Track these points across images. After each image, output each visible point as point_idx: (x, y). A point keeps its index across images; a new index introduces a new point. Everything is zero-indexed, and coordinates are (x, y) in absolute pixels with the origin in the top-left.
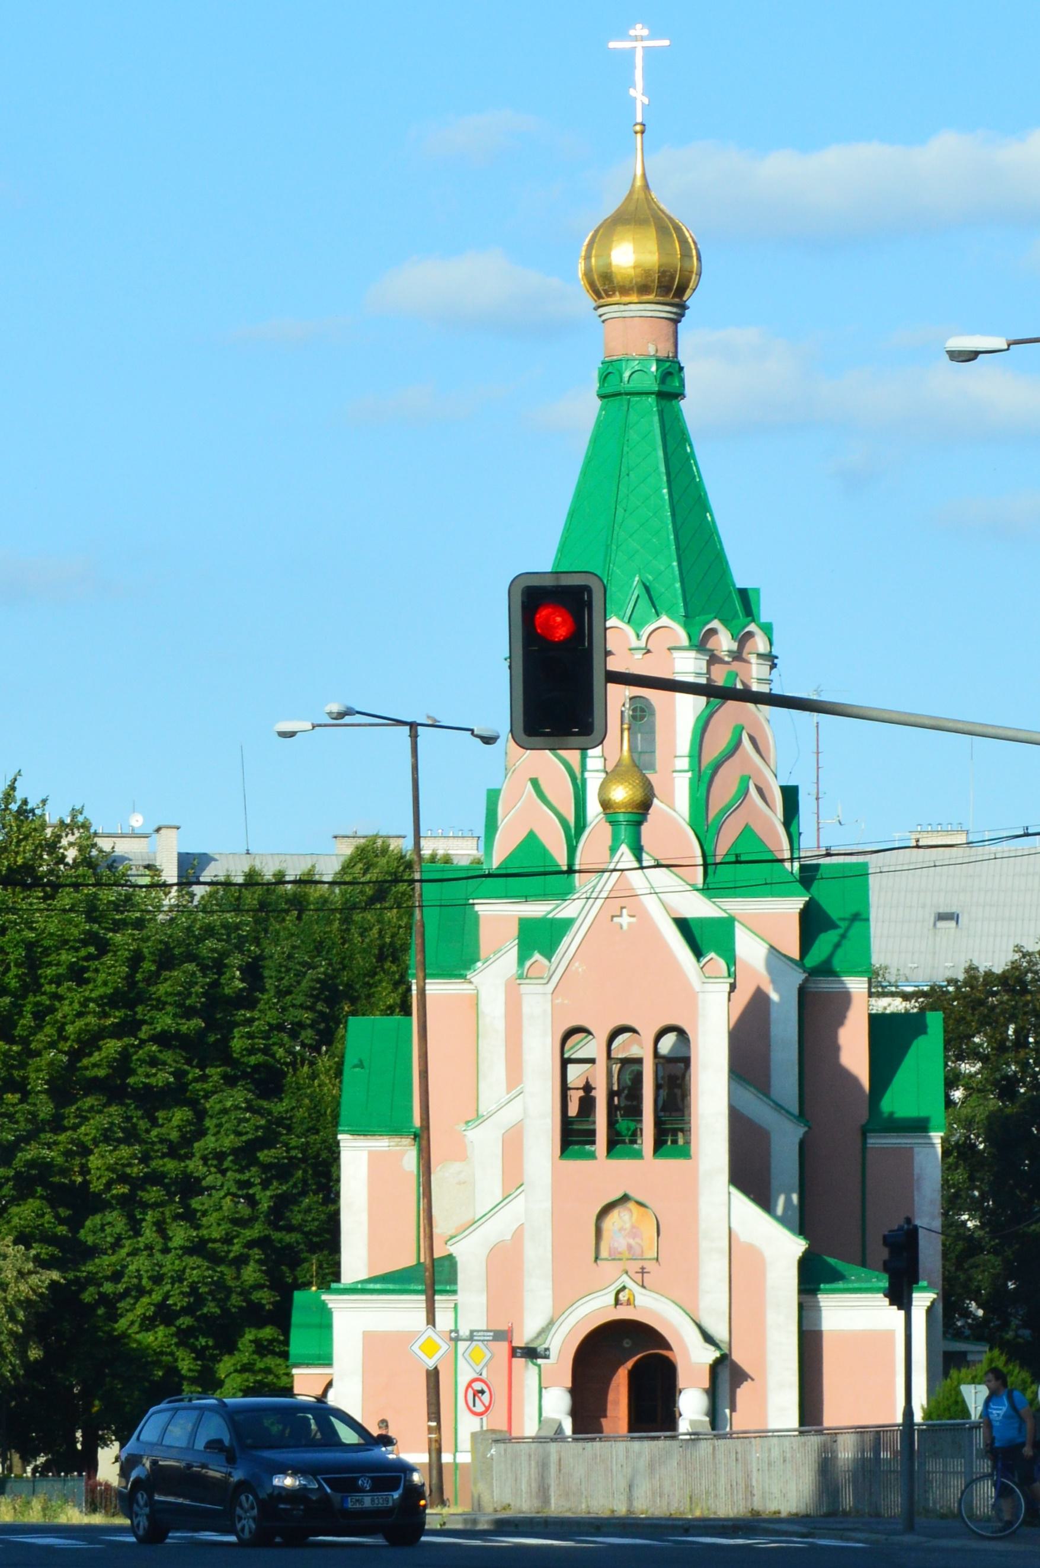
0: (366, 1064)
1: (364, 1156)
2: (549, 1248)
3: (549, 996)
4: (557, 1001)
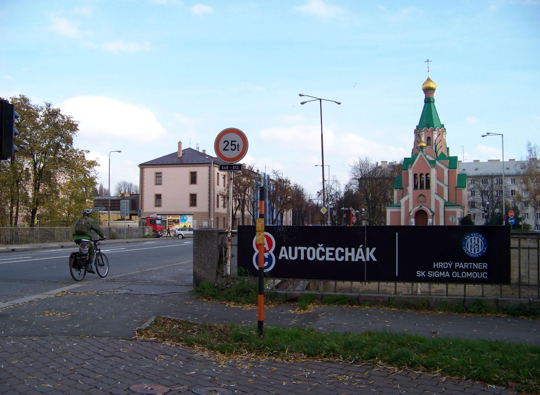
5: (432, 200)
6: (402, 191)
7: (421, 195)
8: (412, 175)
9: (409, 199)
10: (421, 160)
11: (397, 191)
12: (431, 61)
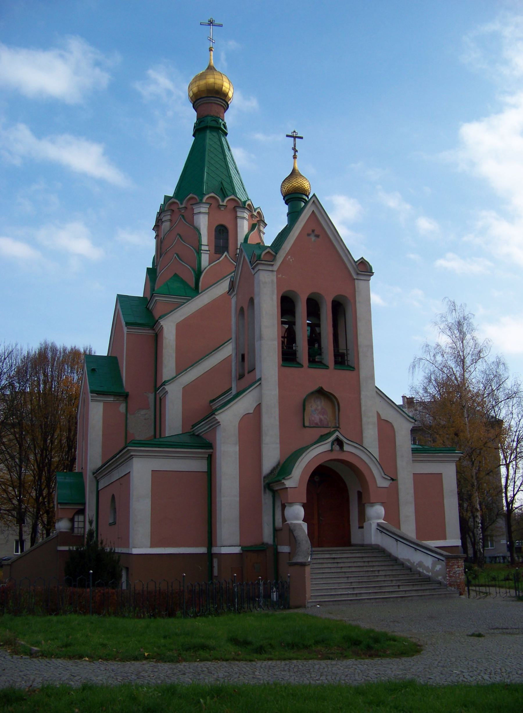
0: (97, 370)
1: (101, 405)
2: (277, 418)
3: (275, 273)
4: (279, 276)
5: (364, 420)
6: (122, 408)
7: (321, 393)
8: (275, 297)
9: (259, 406)
10: (313, 238)
11: (105, 403)
12: (221, 26)
